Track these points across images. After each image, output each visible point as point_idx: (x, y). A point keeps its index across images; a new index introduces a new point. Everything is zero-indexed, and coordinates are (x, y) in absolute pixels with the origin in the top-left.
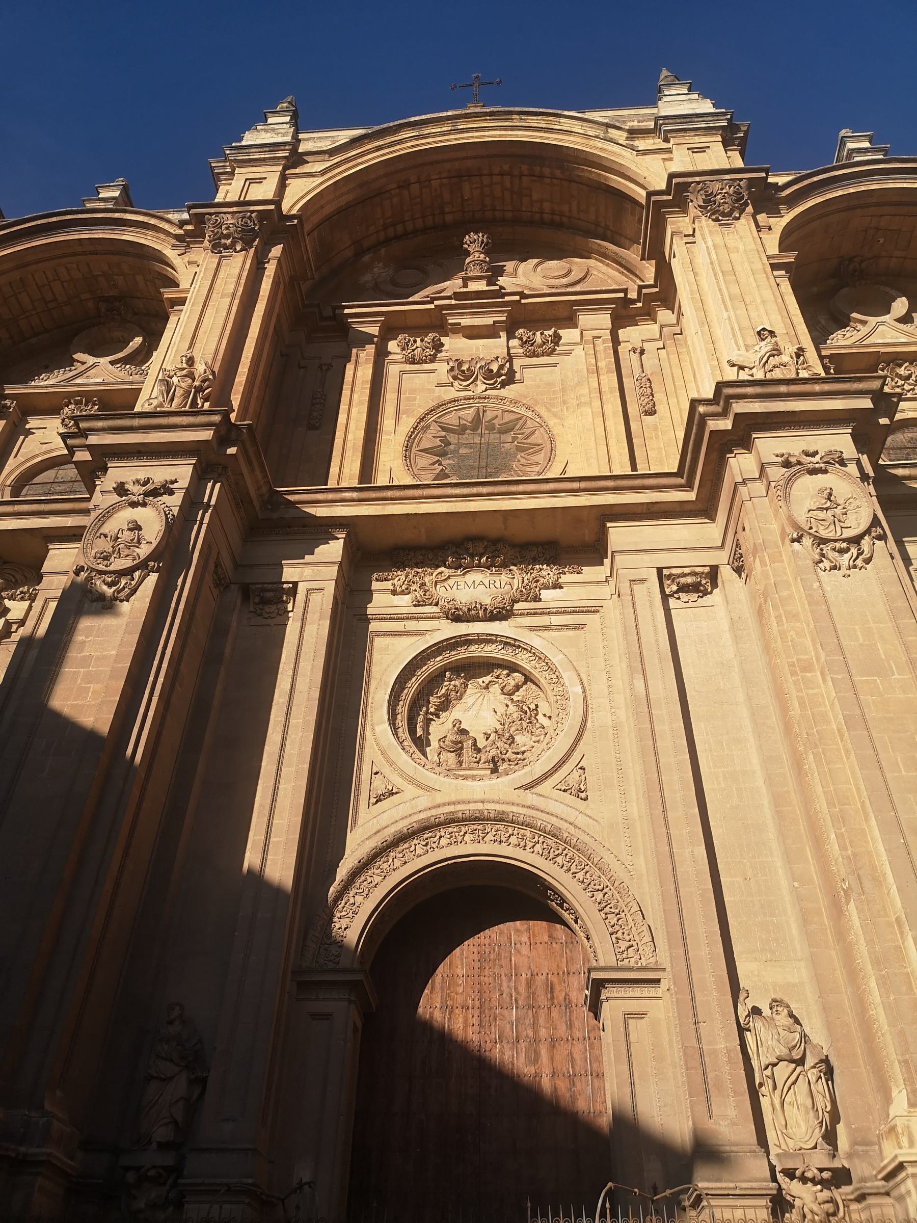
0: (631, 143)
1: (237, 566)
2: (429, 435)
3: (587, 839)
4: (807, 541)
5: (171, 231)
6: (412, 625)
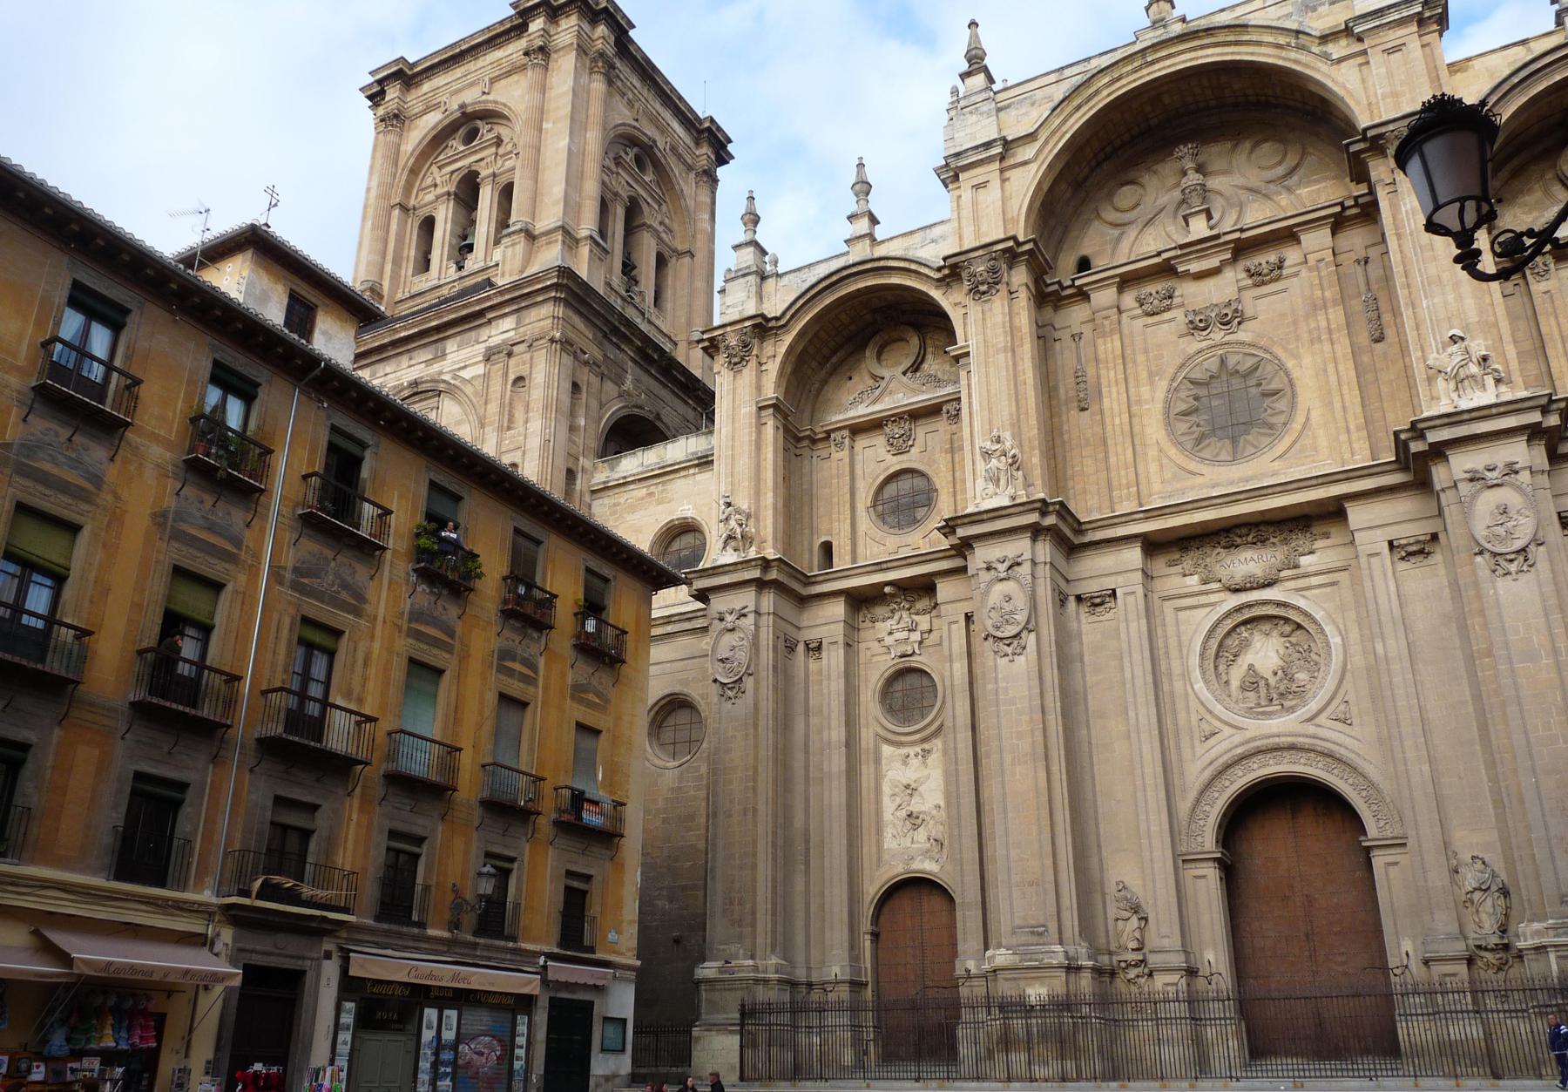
0: (1324, 48)
1: (1068, 581)
2: (1183, 394)
3: (1352, 756)
4: (1487, 555)
5: (932, 274)
6: (1203, 599)
